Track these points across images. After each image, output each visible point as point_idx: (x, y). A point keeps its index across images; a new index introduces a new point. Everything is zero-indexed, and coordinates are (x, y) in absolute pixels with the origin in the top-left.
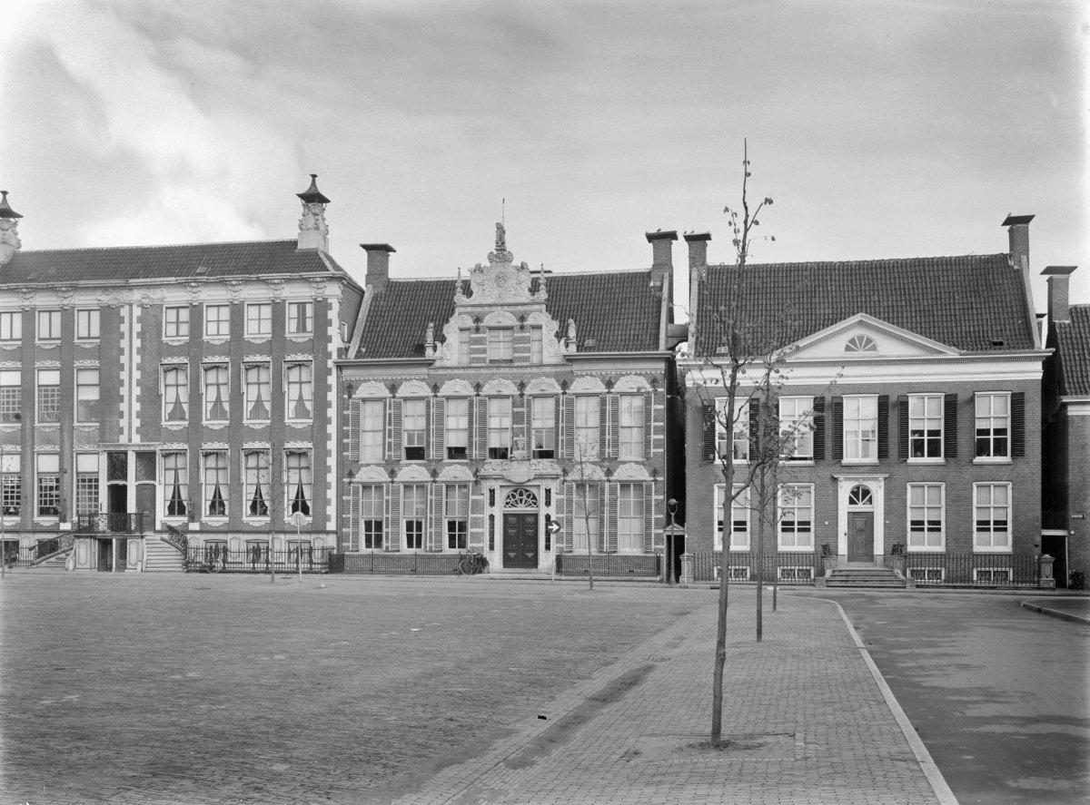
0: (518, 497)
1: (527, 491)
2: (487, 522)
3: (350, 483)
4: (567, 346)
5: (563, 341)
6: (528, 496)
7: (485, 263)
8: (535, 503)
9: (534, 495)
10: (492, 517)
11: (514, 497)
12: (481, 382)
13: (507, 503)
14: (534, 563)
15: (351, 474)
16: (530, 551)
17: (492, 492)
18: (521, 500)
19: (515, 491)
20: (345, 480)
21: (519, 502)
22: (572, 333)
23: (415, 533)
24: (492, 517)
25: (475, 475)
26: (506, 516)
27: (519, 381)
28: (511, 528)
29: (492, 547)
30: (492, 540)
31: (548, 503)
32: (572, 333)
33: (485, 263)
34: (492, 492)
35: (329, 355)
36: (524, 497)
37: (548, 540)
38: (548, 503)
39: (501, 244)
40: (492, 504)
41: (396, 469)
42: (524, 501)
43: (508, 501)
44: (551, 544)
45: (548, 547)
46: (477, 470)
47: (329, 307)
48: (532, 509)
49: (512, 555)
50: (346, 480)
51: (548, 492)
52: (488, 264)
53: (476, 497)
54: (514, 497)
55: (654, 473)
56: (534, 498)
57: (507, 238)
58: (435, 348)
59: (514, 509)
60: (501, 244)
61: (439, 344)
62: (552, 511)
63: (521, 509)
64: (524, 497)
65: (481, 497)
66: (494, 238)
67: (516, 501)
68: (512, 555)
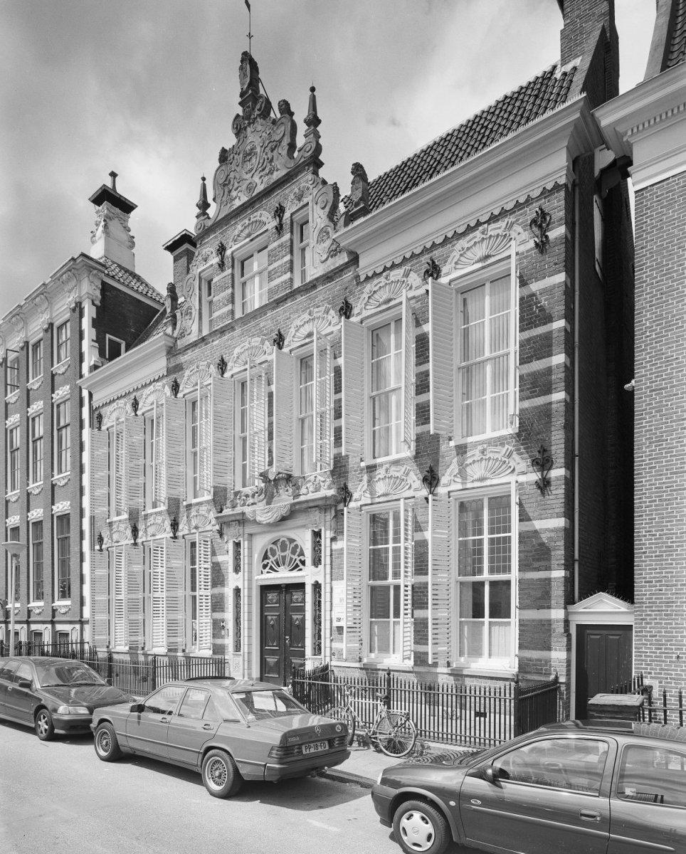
0: (279, 554)
1: (292, 541)
6: (294, 552)
13: (265, 566)
18: (284, 558)
36: (288, 553)
42: (287, 560)
43: (265, 562)
51: (317, 535)
59: (273, 575)
64: (288, 553)
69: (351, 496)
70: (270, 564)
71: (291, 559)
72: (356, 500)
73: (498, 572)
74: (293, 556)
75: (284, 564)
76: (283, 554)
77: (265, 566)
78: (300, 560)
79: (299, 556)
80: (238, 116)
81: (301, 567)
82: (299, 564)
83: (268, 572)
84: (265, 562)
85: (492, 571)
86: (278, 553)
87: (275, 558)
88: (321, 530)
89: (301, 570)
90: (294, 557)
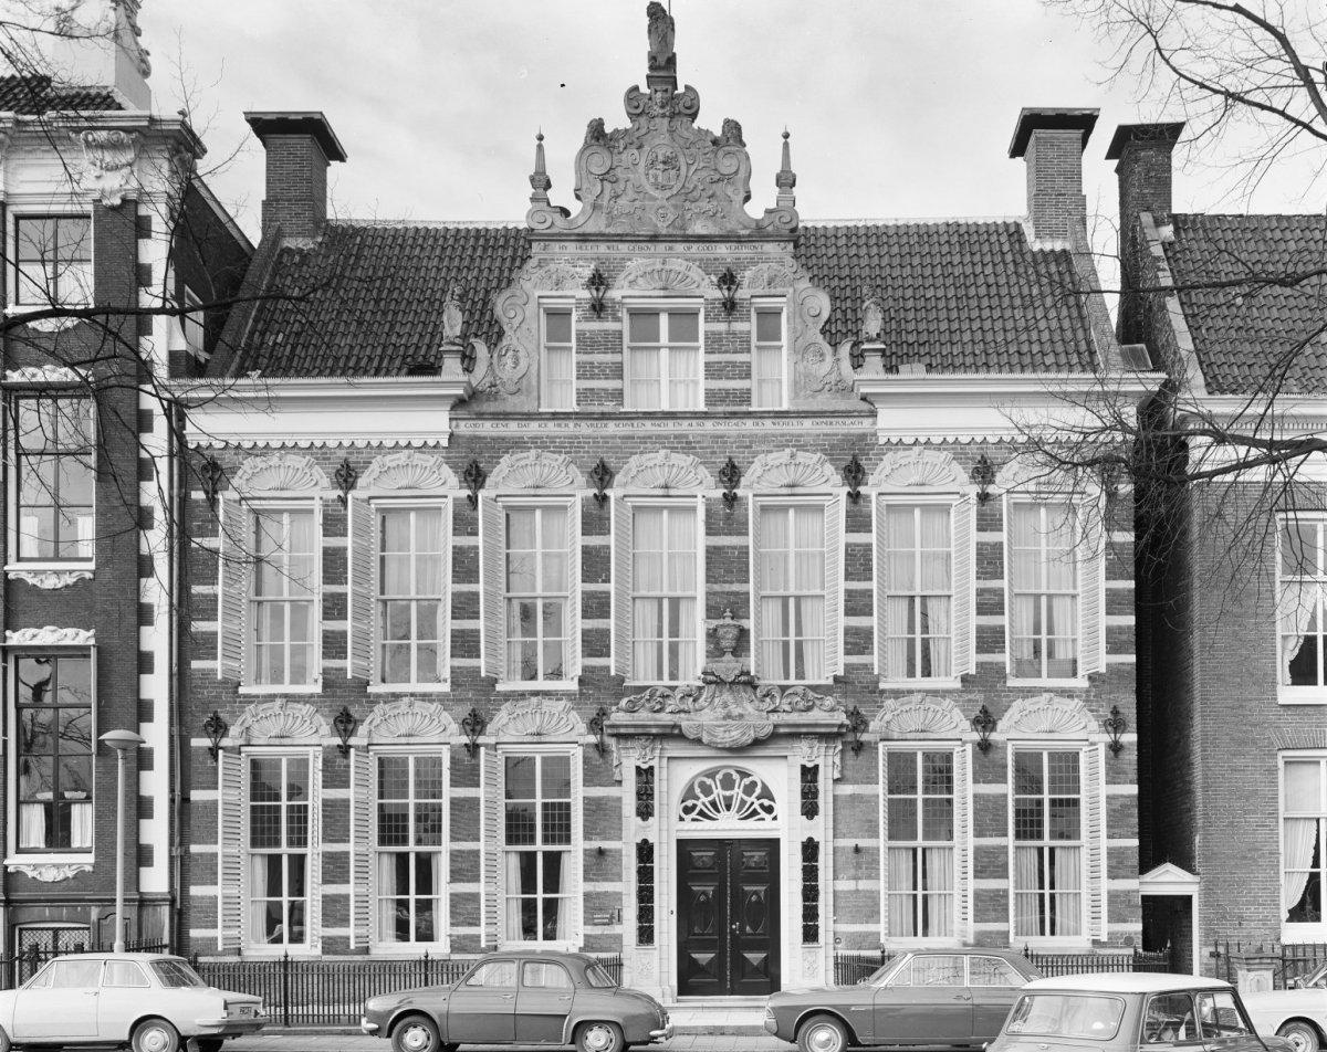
0: (719, 793)
1: (744, 774)
2: (630, 863)
3: (213, 752)
4: (857, 360)
5: (845, 349)
6: (749, 790)
7: (617, 120)
8: (769, 810)
9: (765, 787)
10: (645, 851)
11: (707, 791)
12: (612, 462)
15: (218, 727)
16: (755, 946)
17: (645, 775)
19: (711, 774)
20: (196, 742)
22: (873, 324)
23: (412, 897)
24: (645, 851)
25: (595, 725)
26: (683, 845)
27: (722, 461)
28: (701, 878)
29: (646, 935)
30: (646, 914)
32: (873, 324)
33: (617, 120)
34: (645, 775)
35: (144, 371)
36: (737, 793)
37: (810, 914)
38: (810, 810)
39: (663, 65)
40: (645, 812)
41: (355, 711)
42: (735, 804)
43: (689, 803)
44: (821, 922)
45: (810, 934)
46: (603, 713)
47: (142, 228)
48: (760, 824)
49: (703, 957)
50: (200, 742)
51: (809, 774)
52: (626, 123)
53: (598, 792)
54: (707, 791)
55: (1115, 724)
56: (767, 793)
57: (680, 47)
58: (468, 360)
59: (706, 823)
60: (663, 65)
61: (481, 349)
62: (820, 829)
63: (729, 826)
64: (737, 793)
66: (641, 46)
67: (713, 804)
68: (703, 957)
69: (866, 724)
70: (700, 807)
71: (743, 802)
73: (553, 842)
74: (745, 798)
75: (728, 807)
76: (728, 793)
77: (687, 810)
78: (762, 806)
79: (758, 798)
80: (636, 88)
81: (763, 814)
82: (759, 810)
83: (693, 820)
85: (546, 840)
86: (715, 791)
87: (710, 798)
88: (817, 767)
90: (749, 800)
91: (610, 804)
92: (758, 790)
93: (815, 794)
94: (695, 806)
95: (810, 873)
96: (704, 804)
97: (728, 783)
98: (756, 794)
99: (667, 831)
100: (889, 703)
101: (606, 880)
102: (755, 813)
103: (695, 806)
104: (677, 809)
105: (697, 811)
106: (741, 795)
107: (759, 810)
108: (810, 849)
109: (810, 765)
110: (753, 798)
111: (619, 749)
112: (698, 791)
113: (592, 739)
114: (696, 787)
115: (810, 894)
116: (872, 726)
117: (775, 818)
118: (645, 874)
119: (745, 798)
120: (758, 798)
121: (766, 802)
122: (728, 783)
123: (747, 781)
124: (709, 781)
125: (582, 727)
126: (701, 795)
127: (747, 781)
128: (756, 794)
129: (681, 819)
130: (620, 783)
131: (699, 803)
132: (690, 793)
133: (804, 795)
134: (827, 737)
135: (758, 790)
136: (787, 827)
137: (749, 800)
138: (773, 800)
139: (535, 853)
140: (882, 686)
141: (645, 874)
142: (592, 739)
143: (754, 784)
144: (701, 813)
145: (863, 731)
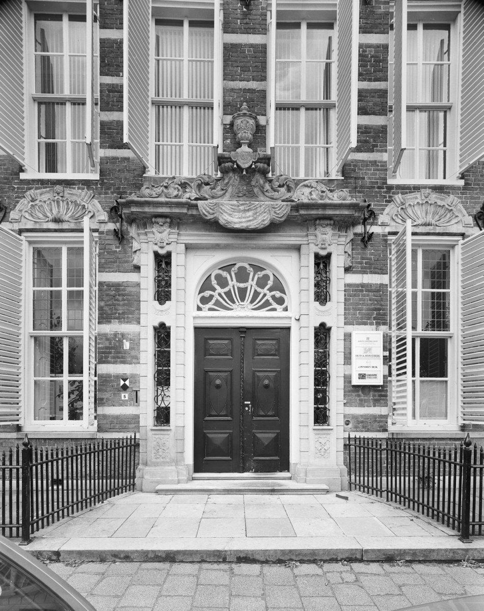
0: (233, 284)
1: (257, 268)
2: (148, 347)
6: (262, 283)
8: (280, 301)
10: (163, 334)
11: (223, 283)
13: (204, 300)
14: (276, 457)
16: (264, 426)
18: (243, 293)
19: (227, 268)
21: (236, 296)
24: (163, 334)
25: (115, 212)
26: (201, 333)
31: (322, 296)
36: (251, 284)
38: (322, 296)
40: (163, 294)
42: (249, 295)
43: (207, 293)
51: (322, 262)
54: (223, 283)
56: (278, 286)
63: (242, 315)
65: (132, 277)
70: (216, 297)
71: (256, 294)
72: (383, 225)
74: (259, 290)
75: (243, 299)
76: (242, 285)
77: (204, 300)
78: (273, 297)
79: (270, 290)
81: (275, 305)
82: (271, 301)
83: (210, 309)
84: (207, 293)
86: (230, 282)
87: (226, 289)
89: (275, 310)
91: (129, 289)
92: (270, 283)
93: (327, 281)
94: (211, 297)
95: (322, 361)
96: (220, 295)
97: (242, 276)
98: (268, 287)
99: (185, 315)
100: (398, 198)
101: (124, 362)
102: (267, 304)
103: (211, 297)
104: (193, 298)
105: (213, 301)
106: (255, 287)
107: (271, 301)
108: (322, 334)
109: (323, 253)
110: (265, 290)
111: (138, 235)
112: (214, 282)
113: (111, 226)
114: (213, 278)
115: (321, 379)
116: (382, 218)
117: (286, 309)
118: (163, 358)
119: (259, 290)
120: (270, 290)
121: (278, 294)
122: (242, 276)
123: (261, 274)
124: (225, 274)
125: (104, 216)
126: (217, 287)
127: (261, 274)
128: (268, 287)
129: (199, 309)
130: (137, 268)
131: (216, 294)
132: (206, 285)
133: (317, 285)
134: (342, 224)
135: (270, 283)
136: (299, 314)
137: (262, 291)
138: (283, 291)
139: (61, 339)
140: (390, 182)
141: (163, 358)
142: (111, 226)
143: (266, 277)
144: (218, 303)
145: (372, 224)
